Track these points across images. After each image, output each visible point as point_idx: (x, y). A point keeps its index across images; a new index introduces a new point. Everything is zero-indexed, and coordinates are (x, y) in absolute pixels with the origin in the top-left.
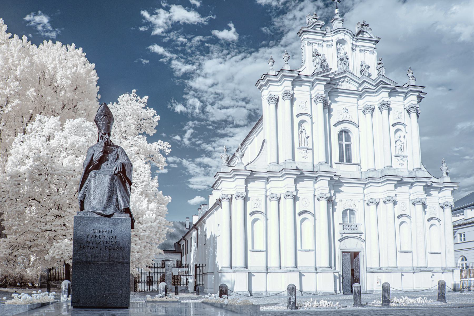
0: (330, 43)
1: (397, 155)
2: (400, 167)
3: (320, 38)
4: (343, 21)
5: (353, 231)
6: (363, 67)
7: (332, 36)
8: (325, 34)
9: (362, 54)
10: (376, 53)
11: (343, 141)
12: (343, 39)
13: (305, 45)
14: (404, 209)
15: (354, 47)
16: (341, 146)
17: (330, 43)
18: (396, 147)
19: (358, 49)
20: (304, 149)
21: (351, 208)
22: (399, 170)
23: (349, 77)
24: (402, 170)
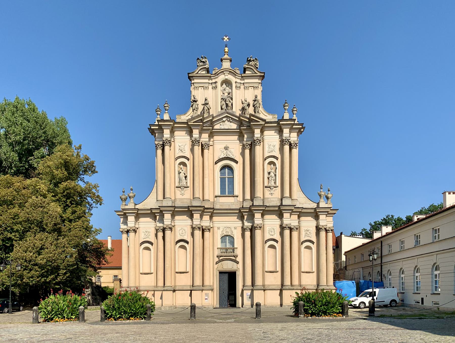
0: (214, 85)
1: (269, 186)
2: (270, 196)
3: (206, 81)
4: (231, 61)
5: (230, 254)
6: (245, 105)
7: (217, 78)
8: (210, 77)
9: (246, 91)
10: (261, 88)
11: (225, 176)
12: (226, 79)
13: (191, 90)
14: (273, 233)
15: (238, 85)
16: (223, 180)
17: (214, 85)
18: (268, 178)
19: (242, 87)
20: (181, 188)
21: (227, 234)
22: (269, 200)
23: (230, 117)
24: (271, 199)
